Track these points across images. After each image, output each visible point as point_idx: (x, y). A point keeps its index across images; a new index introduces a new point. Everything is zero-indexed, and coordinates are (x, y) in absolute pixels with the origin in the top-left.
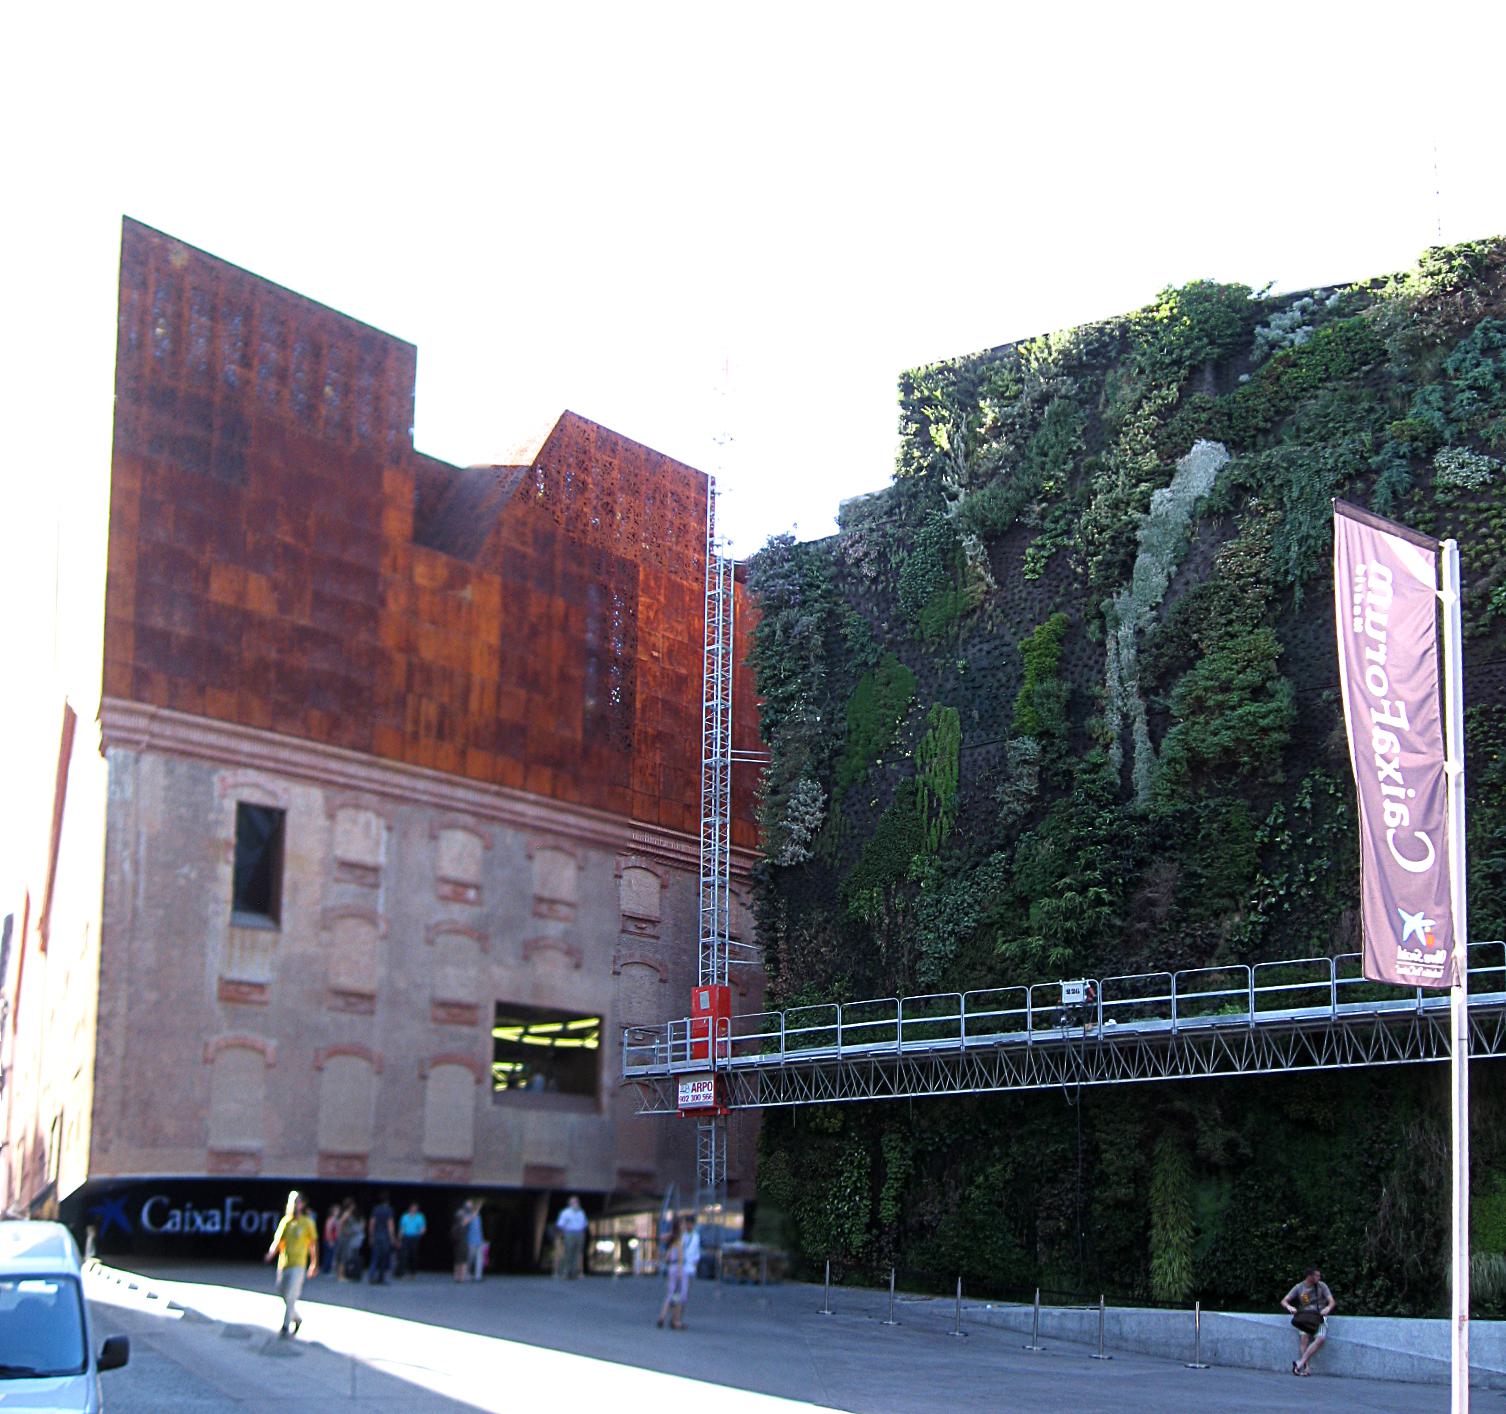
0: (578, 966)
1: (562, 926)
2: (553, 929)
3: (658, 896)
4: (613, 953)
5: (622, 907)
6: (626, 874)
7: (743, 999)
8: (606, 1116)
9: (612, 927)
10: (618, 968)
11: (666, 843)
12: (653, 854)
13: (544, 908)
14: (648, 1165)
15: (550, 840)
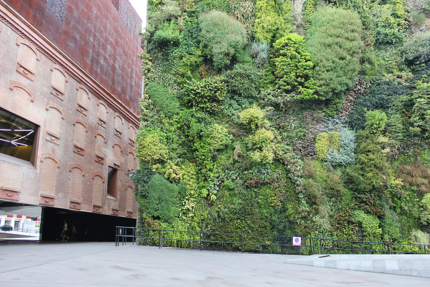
0: (32, 101)
1: (28, 81)
2: (24, 81)
3: (64, 84)
4: (46, 100)
5: (52, 84)
6: (55, 71)
7: (86, 133)
8: (38, 171)
9: (47, 90)
10: (48, 108)
11: (69, 64)
12: (65, 67)
13: (21, 70)
14: (51, 194)
15: (28, 43)
